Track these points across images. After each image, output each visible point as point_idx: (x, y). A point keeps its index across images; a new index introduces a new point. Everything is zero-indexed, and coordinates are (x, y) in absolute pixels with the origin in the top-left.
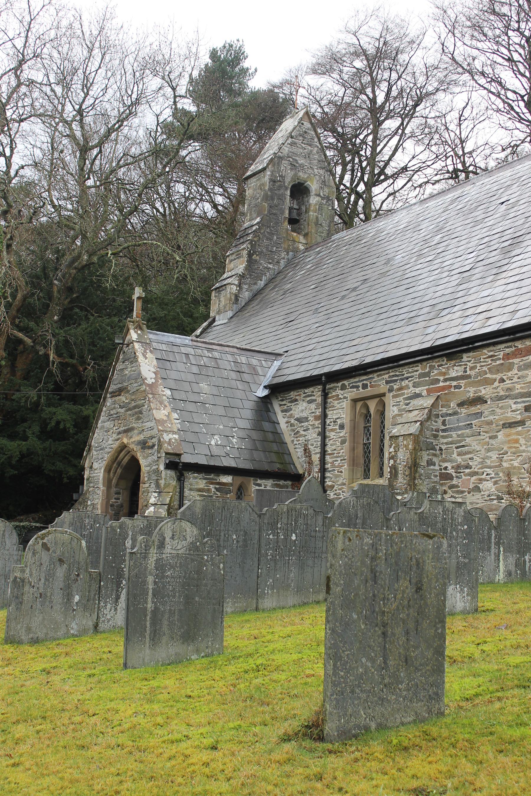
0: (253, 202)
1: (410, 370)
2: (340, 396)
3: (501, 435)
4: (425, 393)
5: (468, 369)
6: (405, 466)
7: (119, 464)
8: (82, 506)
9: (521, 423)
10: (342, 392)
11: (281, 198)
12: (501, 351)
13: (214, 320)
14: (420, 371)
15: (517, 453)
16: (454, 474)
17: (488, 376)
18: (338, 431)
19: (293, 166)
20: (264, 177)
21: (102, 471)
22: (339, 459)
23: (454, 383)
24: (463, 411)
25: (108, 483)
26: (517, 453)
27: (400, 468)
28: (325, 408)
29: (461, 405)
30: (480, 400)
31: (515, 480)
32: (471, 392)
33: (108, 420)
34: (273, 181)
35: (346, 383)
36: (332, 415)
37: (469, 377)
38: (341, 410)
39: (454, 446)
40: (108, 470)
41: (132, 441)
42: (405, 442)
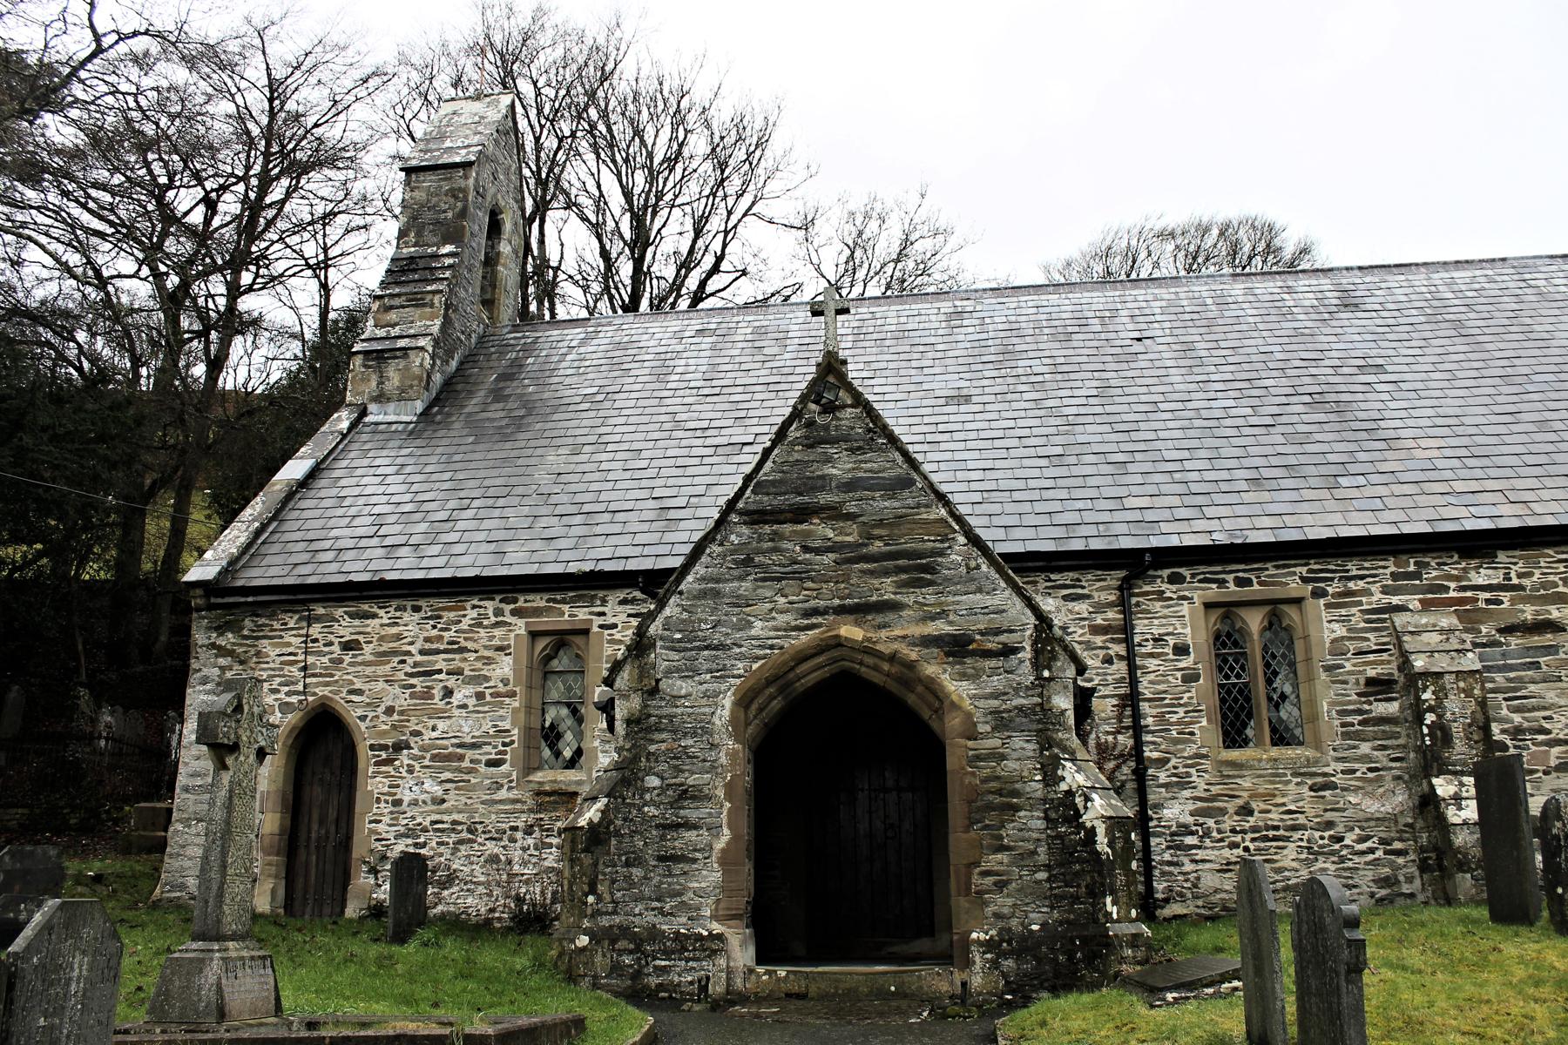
0: (428, 216)
1: (1367, 565)
2: (1168, 594)
4: (1415, 604)
5: (1513, 575)
6: (1470, 725)
7: (781, 691)
8: (632, 789)
10: (1174, 588)
13: (364, 412)
14: (1393, 569)
16: (1509, 742)
17: (1561, 589)
18: (1171, 657)
20: (466, 177)
21: (728, 701)
22: (1181, 710)
23: (1487, 595)
24: (1515, 642)
27: (1457, 729)
29: (1508, 630)
32: (1528, 613)
33: (741, 578)
36: (1140, 626)
37: (1521, 588)
38: (1177, 616)
39: (1500, 696)
40: (744, 701)
41: (897, 636)
42: (1462, 684)
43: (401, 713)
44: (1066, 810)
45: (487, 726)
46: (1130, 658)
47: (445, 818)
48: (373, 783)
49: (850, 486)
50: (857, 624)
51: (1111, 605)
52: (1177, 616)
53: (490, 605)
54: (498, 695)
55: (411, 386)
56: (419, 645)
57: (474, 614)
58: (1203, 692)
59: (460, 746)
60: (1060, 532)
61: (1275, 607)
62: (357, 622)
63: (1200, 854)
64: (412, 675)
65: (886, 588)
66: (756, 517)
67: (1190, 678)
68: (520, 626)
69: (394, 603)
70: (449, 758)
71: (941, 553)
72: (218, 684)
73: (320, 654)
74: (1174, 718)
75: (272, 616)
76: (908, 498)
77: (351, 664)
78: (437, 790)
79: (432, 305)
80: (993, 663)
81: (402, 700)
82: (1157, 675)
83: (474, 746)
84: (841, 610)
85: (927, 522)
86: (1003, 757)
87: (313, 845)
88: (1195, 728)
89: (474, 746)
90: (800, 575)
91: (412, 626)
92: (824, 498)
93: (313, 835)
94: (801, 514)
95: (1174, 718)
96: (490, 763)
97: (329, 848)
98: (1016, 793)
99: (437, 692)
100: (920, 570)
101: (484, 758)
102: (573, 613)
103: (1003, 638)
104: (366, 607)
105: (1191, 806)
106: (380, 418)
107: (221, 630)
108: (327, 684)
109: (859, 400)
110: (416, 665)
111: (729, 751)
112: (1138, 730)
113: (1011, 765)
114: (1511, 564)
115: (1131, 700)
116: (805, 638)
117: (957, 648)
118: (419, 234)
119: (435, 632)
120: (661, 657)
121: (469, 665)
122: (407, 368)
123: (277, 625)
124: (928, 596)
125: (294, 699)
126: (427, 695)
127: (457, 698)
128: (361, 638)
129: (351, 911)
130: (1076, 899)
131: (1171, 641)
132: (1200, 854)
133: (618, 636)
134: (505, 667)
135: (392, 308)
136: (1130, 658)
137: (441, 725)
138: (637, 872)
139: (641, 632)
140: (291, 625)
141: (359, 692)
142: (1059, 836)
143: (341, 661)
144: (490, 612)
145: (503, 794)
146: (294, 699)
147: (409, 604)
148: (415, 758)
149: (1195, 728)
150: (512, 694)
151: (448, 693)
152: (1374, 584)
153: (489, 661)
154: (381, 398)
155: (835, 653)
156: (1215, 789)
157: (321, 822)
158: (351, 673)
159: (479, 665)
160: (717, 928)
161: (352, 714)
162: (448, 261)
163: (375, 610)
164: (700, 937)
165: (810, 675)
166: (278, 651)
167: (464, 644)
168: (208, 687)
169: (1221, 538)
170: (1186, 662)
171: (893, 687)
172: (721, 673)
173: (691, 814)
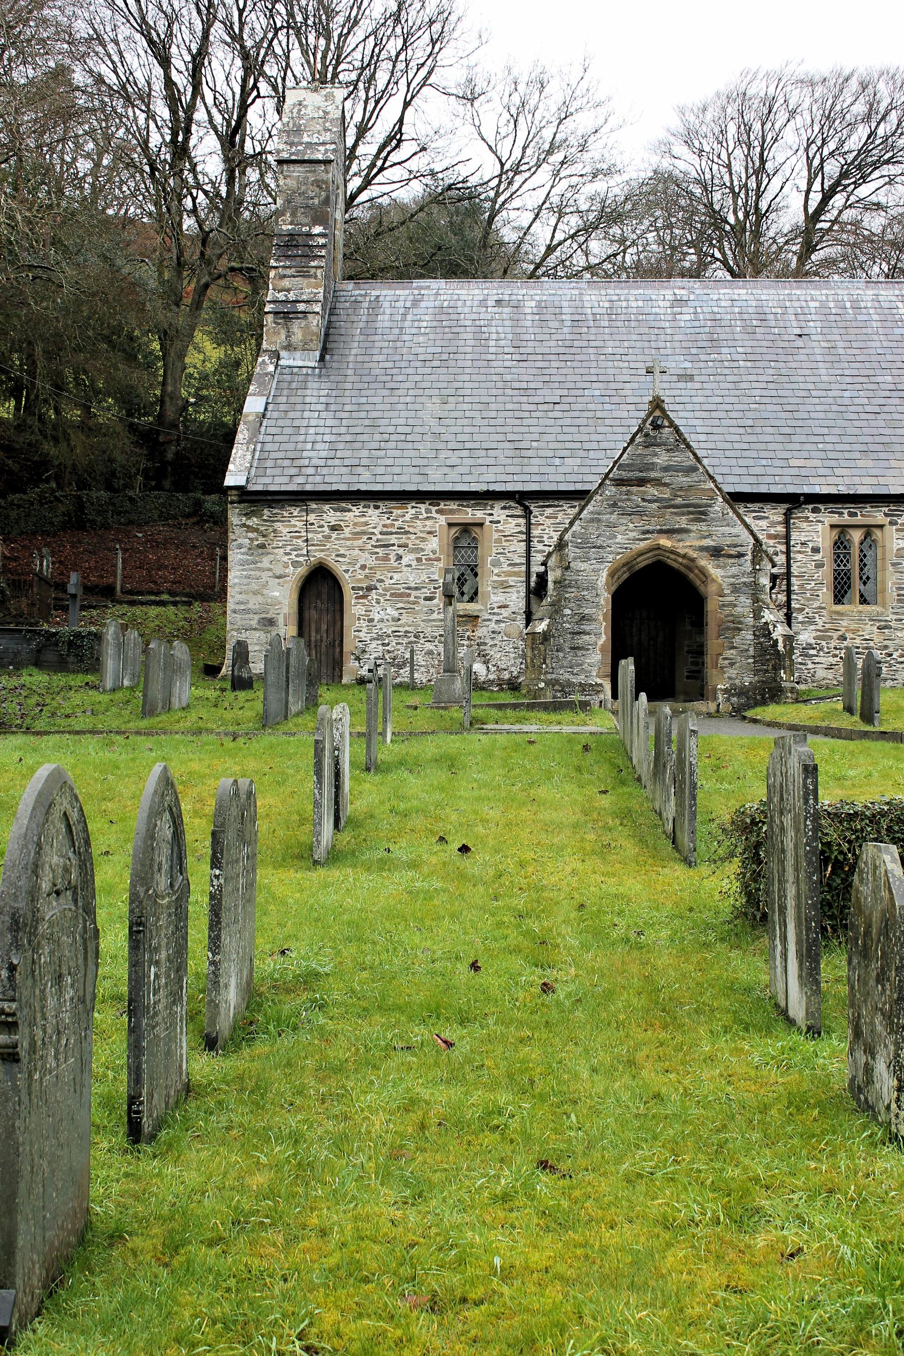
0: (299, 200)
7: (629, 569)
21: (605, 574)
22: (813, 583)
28: (788, 528)
33: (611, 513)
35: (820, 506)
36: (795, 536)
40: (612, 575)
41: (687, 545)
43: (371, 569)
44: (765, 631)
45: (424, 577)
46: (788, 553)
47: (400, 629)
48: (354, 608)
49: (666, 469)
50: (668, 539)
51: (780, 523)
52: (815, 531)
53: (423, 507)
54: (430, 560)
55: (312, 340)
56: (380, 528)
57: (413, 511)
58: (826, 574)
59: (409, 588)
60: (753, 480)
61: (868, 530)
62: (338, 514)
63: (817, 660)
64: (376, 547)
65: (682, 522)
67: (820, 565)
68: (442, 520)
69: (363, 504)
70: (401, 595)
71: (710, 506)
72: (250, 549)
73: (316, 532)
74: (809, 587)
75: (282, 508)
76: (695, 477)
77: (337, 539)
78: (396, 614)
79: (316, 277)
80: (733, 561)
81: (371, 562)
82: (802, 563)
83: (416, 589)
84: (661, 532)
85: (704, 490)
86: (735, 606)
87: (313, 645)
88: (820, 593)
89: (416, 589)
90: (640, 513)
91: (374, 517)
92: (653, 475)
93: (313, 639)
94: (641, 482)
95: (809, 587)
96: (426, 599)
97: (323, 646)
98: (740, 623)
99: (392, 557)
100: (700, 513)
101: (423, 596)
102: (472, 514)
103: (738, 549)
104: (344, 505)
105: (814, 634)
106: (291, 363)
108: (322, 551)
109: (672, 424)
110: (378, 540)
111: (605, 599)
113: (739, 609)
116: (642, 545)
117: (716, 552)
118: (293, 215)
119: (389, 522)
120: (571, 551)
121: (411, 541)
122: (307, 327)
123: (286, 514)
124: (703, 526)
125: (301, 559)
126: (386, 558)
127: (405, 561)
128: (342, 523)
129: (344, 681)
130: (767, 671)
131: (811, 545)
132: (817, 660)
133: (501, 528)
134: (433, 543)
135: (285, 276)
136: (788, 553)
137: (396, 576)
138: (561, 654)
139: (561, 539)
140: (295, 514)
141: (343, 556)
142: (760, 643)
143: (330, 537)
144: (423, 511)
145: (435, 616)
146: (301, 559)
147: (372, 504)
148: (381, 595)
149: (820, 593)
150: (438, 560)
151: (400, 558)
153: (423, 540)
154: (289, 347)
155: (656, 552)
156: (828, 626)
157: (318, 631)
158: (336, 543)
159: (417, 542)
160: (599, 681)
161: (339, 568)
162: (322, 241)
163: (350, 506)
164: (591, 685)
165: (642, 562)
166: (288, 530)
167: (407, 529)
168: (242, 550)
169: (844, 490)
170: (818, 557)
171: (682, 569)
172: (601, 560)
173: (587, 628)
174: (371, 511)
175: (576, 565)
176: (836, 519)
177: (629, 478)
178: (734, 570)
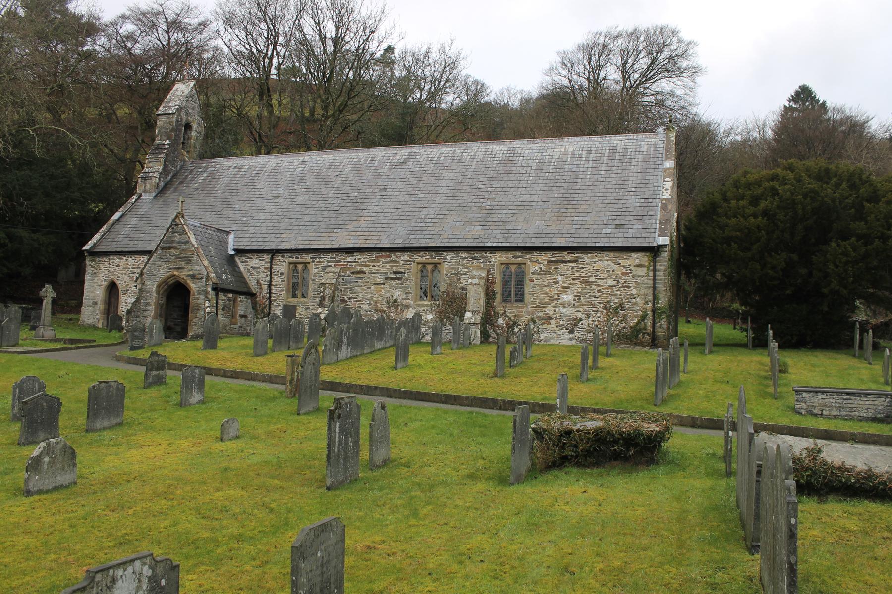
0: (163, 130)
3: (372, 287)
9: (383, 284)
11: (180, 131)
12: (374, 255)
13: (141, 195)
15: (381, 295)
19: (187, 114)
25: (158, 292)
26: (381, 295)
27: (327, 297)
28: (271, 264)
29: (353, 273)
30: (363, 272)
31: (379, 305)
32: (358, 269)
34: (177, 121)
36: (275, 268)
38: (282, 265)
40: (158, 286)
41: (183, 275)
46: (271, 275)
49: (179, 242)
52: (282, 265)
61: (306, 264)
65: (183, 264)
66: (163, 248)
67: (283, 281)
76: (188, 245)
81: (128, 280)
82: (276, 279)
90: (169, 261)
94: (170, 248)
107: (92, 261)
112: (270, 293)
114: (357, 256)
115: (270, 285)
117: (193, 277)
120: (145, 277)
124: (189, 266)
136: (271, 275)
139: (142, 271)
152: (325, 259)
154: (145, 191)
161: (118, 282)
165: (171, 281)
172: (154, 280)
174: (130, 259)
175: (147, 283)
176: (291, 260)
177: (166, 246)
178: (199, 285)
